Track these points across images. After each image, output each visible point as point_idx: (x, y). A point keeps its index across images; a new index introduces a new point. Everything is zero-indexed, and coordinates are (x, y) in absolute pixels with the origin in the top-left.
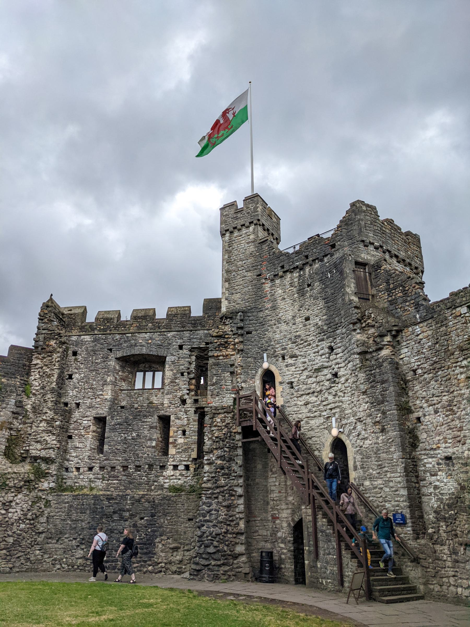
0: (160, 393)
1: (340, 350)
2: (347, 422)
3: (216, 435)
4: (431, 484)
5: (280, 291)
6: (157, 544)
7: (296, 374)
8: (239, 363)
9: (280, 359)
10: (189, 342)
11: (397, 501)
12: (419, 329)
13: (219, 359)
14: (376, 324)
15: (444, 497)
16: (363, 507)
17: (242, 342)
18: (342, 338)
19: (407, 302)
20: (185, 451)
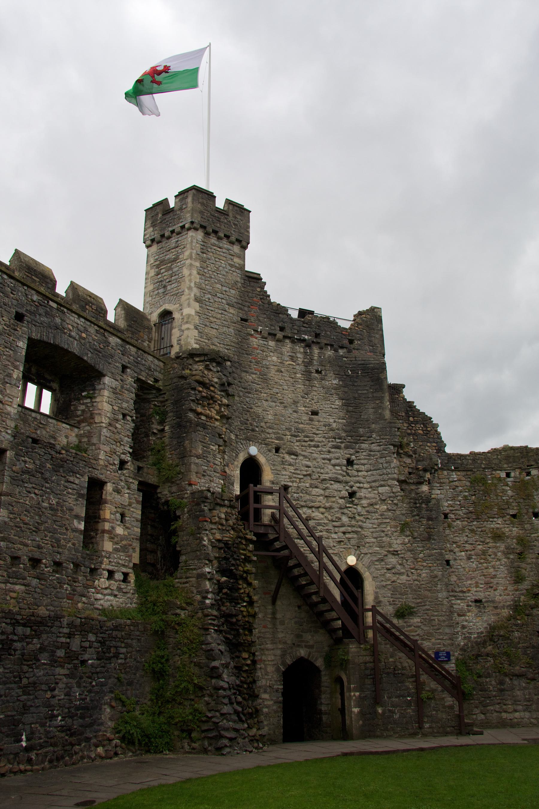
0: (74, 435)
1: (362, 468)
2: (367, 552)
3: (218, 536)
4: (458, 623)
5: (275, 359)
6: (104, 707)
7: (295, 478)
8: (223, 436)
9: (274, 451)
10: (135, 366)
12: (455, 476)
13: (200, 418)
16: (388, 646)
17: (228, 406)
18: (369, 455)
19: (428, 442)
20: (124, 549)
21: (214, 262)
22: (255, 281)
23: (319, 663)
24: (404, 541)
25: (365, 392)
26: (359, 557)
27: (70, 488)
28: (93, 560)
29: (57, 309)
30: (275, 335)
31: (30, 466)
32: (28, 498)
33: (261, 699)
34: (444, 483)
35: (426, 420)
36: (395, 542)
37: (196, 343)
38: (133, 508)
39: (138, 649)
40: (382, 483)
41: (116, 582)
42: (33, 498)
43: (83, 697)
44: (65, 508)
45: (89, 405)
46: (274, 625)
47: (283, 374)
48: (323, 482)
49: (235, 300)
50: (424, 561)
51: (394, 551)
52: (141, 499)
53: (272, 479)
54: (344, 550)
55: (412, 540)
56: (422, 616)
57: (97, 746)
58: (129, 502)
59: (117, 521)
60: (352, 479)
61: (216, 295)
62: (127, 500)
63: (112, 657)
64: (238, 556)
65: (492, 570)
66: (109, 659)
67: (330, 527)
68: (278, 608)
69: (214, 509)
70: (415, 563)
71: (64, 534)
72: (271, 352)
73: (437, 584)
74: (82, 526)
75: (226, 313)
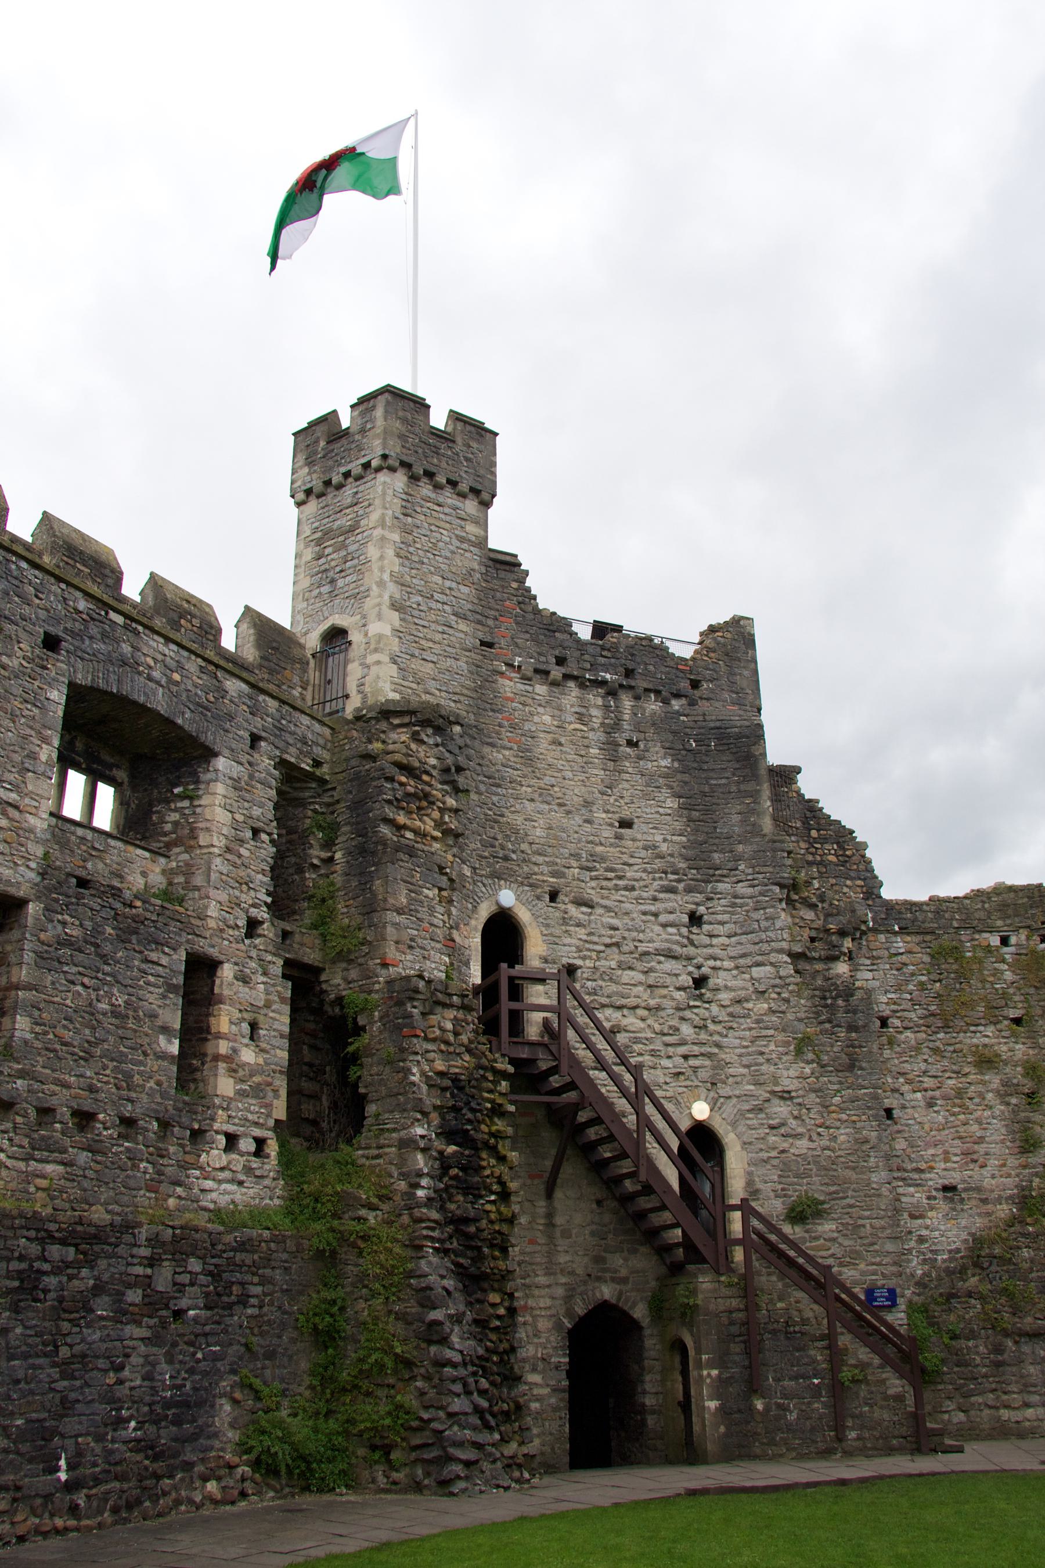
0: (158, 870)
1: (719, 929)
2: (731, 1094)
3: (440, 1065)
4: (910, 1232)
5: (547, 719)
7: (589, 950)
8: (448, 870)
9: (547, 898)
10: (276, 736)
11: (873, 1264)
12: (901, 944)
13: (403, 836)
14: (820, 905)
15: (939, 1257)
16: (774, 1278)
17: (456, 811)
18: (733, 905)
19: (847, 879)
20: (257, 1091)
21: (428, 533)
22: (507, 568)
23: (640, 1312)
24: (802, 1072)
25: (723, 781)
26: (715, 1104)
27: (152, 975)
28: (196, 1113)
29: (125, 627)
30: (547, 673)
31: (75, 932)
32: (70, 995)
33: (525, 1383)
34: (879, 958)
35: (842, 836)
36: (785, 1073)
37: (394, 691)
38: (273, 1011)
39: (285, 1287)
40: (759, 958)
41: (242, 1156)
42: (80, 994)
43: (179, 1382)
44: (141, 1013)
45: (187, 811)
46: (551, 1238)
47: (564, 749)
48: (643, 958)
49: (470, 606)
50: (842, 1110)
51: (784, 1091)
52: (288, 994)
53: (544, 954)
54: (685, 1089)
55: (818, 1069)
56: (840, 1218)
57: (205, 1479)
58: (267, 1000)
59: (244, 1037)
60: (699, 951)
61: (432, 596)
62: (263, 996)
63: (234, 1303)
64: (479, 1104)
65: (975, 1127)
66: (230, 1306)
67: (658, 1046)
68: (557, 1204)
69: (431, 1013)
70: (825, 1115)
71: (140, 1063)
72: (540, 705)
73: (869, 1156)
74: (174, 1048)
75: (451, 631)
